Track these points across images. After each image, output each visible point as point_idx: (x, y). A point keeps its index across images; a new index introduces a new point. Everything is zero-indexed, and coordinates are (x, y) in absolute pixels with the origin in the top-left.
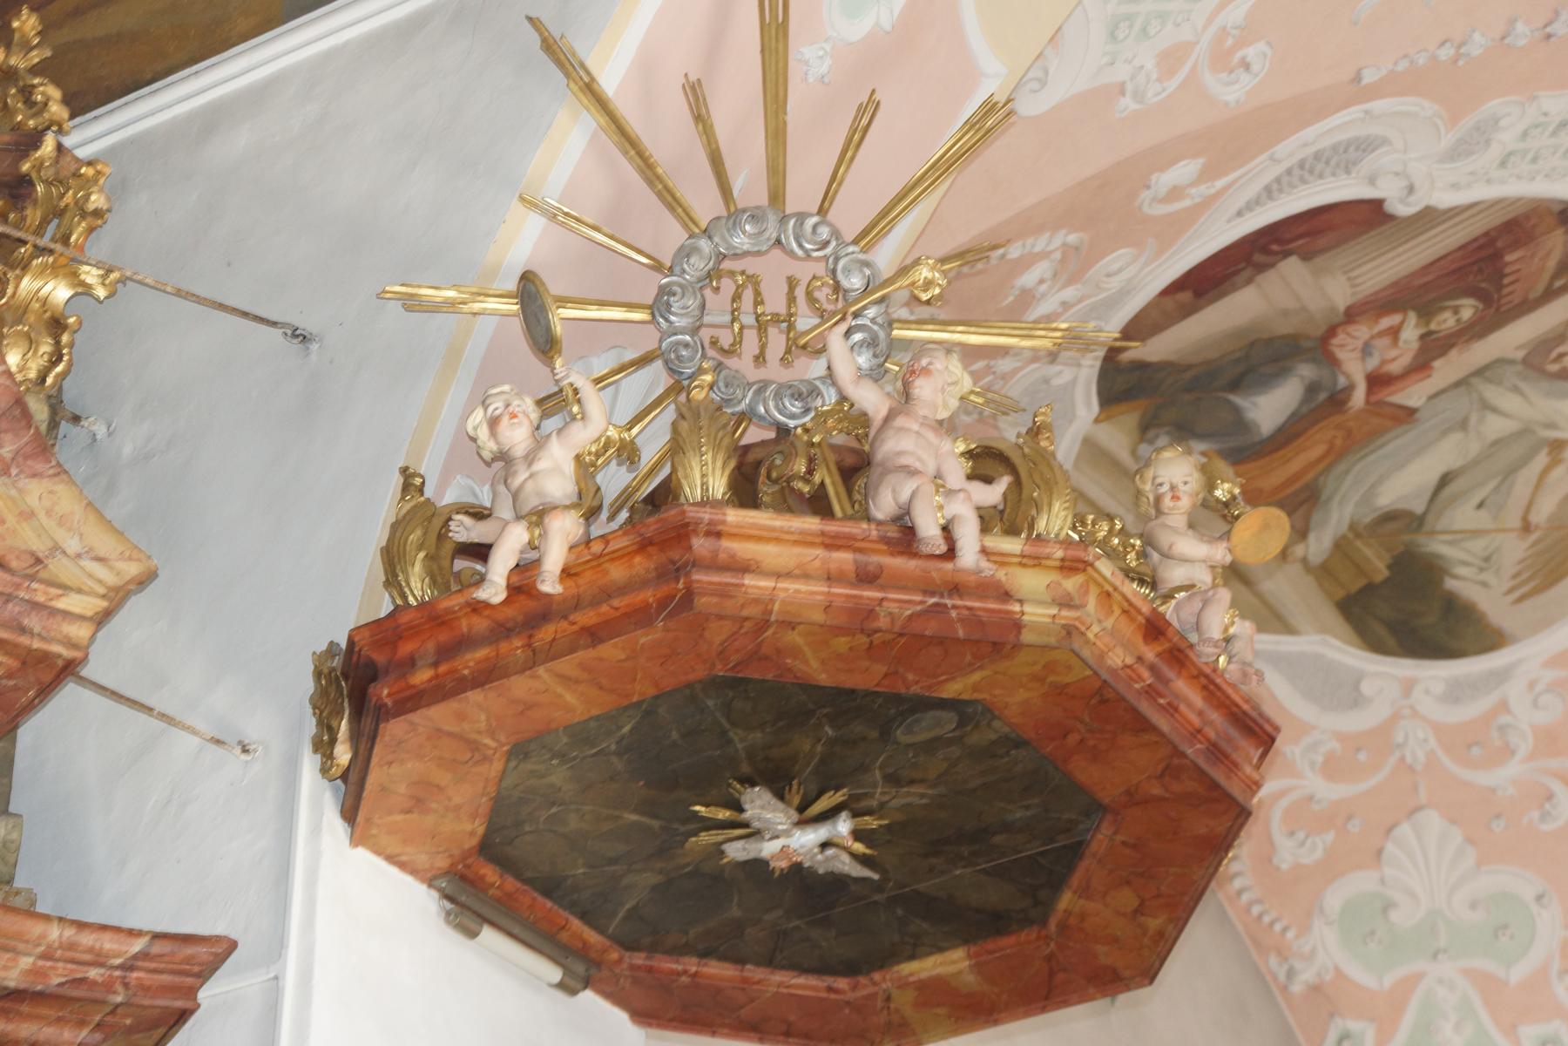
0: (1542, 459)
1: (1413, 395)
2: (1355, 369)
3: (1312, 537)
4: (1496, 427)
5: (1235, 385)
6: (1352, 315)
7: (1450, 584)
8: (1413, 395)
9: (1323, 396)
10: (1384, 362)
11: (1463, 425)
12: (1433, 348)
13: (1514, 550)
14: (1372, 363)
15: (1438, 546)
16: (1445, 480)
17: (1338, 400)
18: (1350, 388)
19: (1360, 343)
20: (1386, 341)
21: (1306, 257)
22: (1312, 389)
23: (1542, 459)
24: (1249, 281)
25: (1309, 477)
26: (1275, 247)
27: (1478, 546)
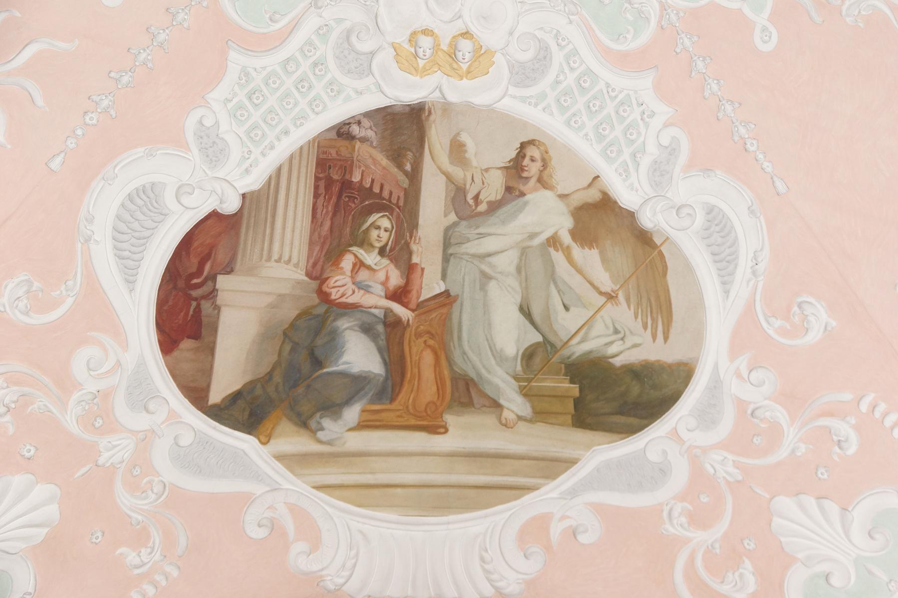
0: (558, 257)
1: (431, 285)
2: (375, 300)
3: (502, 402)
4: (506, 262)
5: (318, 363)
6: (318, 275)
7: (618, 362)
8: (431, 285)
9: (380, 328)
10: (384, 284)
11: (486, 278)
12: (399, 252)
13: (623, 314)
14: (379, 289)
15: (579, 349)
16: (526, 311)
17: (393, 324)
18: (388, 311)
19: (351, 286)
20: (363, 275)
21: (229, 270)
22: (367, 329)
23: (558, 257)
24: (218, 308)
25: (446, 373)
26: (195, 281)
27: (599, 328)
